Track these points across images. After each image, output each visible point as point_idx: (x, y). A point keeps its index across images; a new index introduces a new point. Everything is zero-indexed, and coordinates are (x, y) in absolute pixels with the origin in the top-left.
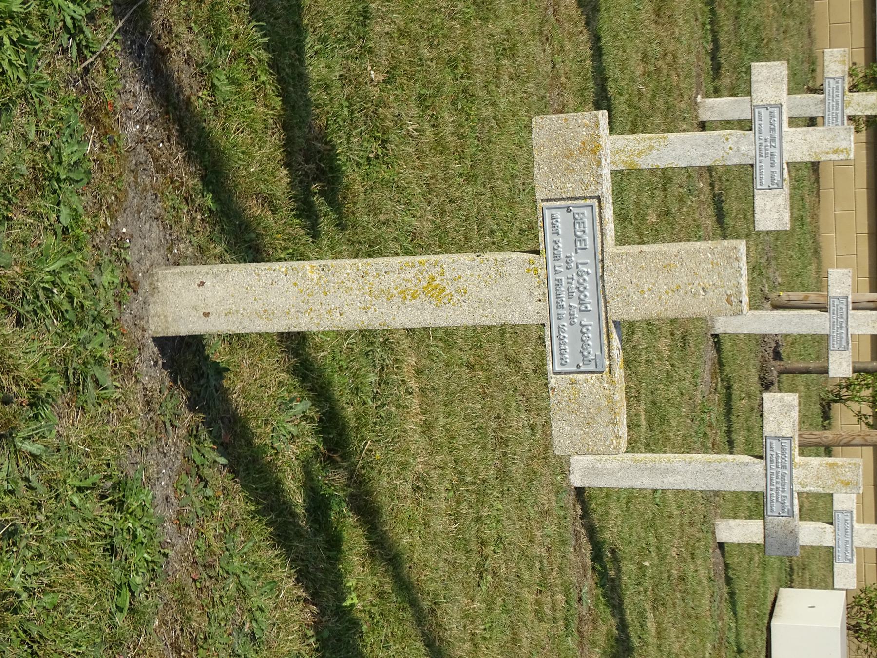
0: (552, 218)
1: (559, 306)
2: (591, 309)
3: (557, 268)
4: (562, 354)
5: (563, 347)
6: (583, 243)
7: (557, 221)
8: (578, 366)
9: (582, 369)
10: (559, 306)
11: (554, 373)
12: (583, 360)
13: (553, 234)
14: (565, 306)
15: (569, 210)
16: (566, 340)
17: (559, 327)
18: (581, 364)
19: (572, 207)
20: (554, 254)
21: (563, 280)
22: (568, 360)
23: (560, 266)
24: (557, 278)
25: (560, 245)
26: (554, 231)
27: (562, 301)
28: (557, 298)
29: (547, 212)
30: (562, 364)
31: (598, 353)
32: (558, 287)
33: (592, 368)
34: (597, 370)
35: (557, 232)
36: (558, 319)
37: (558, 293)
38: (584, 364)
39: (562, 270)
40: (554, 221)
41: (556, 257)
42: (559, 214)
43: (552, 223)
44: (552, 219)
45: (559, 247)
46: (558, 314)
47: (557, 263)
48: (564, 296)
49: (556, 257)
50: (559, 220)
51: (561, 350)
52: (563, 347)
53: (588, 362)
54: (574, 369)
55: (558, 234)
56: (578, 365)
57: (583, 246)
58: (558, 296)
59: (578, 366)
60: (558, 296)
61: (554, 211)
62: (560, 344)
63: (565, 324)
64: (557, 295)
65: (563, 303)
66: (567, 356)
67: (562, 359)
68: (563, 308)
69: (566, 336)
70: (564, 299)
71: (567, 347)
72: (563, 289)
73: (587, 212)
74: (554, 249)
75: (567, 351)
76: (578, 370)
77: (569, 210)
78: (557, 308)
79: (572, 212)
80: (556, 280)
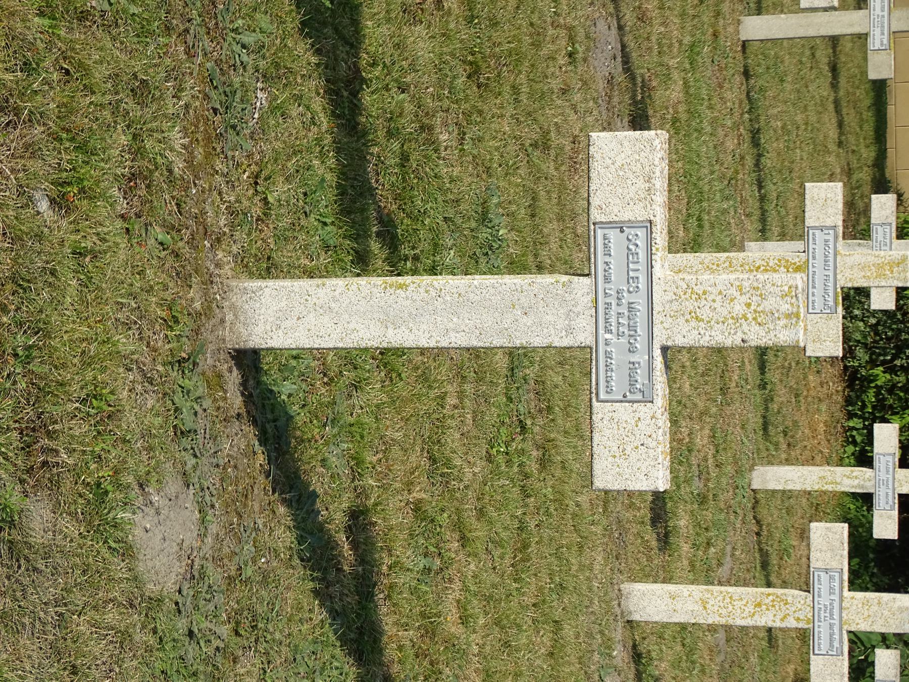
0: (605, 238)
2: (641, 333)
3: (607, 291)
4: (607, 382)
5: (609, 374)
6: (636, 256)
7: (610, 242)
8: (625, 396)
9: (630, 397)
11: (598, 401)
13: (605, 255)
14: (613, 331)
15: (622, 231)
18: (628, 394)
20: (605, 276)
21: (613, 304)
22: (614, 388)
23: (610, 289)
24: (607, 301)
25: (612, 266)
27: (611, 325)
29: (600, 233)
30: (607, 392)
31: (647, 382)
34: (645, 399)
36: (606, 344)
37: (607, 317)
38: (630, 392)
41: (607, 279)
42: (613, 234)
43: (605, 244)
44: (605, 239)
47: (607, 286)
48: (613, 320)
50: (611, 241)
51: (607, 377)
52: (609, 374)
54: (621, 398)
55: (610, 255)
56: (625, 394)
57: (635, 260)
58: (606, 321)
59: (624, 397)
60: (606, 321)
61: (606, 231)
62: (607, 371)
63: (613, 350)
64: (606, 319)
66: (613, 384)
67: (607, 387)
69: (613, 362)
70: (613, 324)
71: (613, 374)
73: (641, 233)
74: (605, 271)
75: (614, 378)
77: (622, 231)
79: (625, 235)
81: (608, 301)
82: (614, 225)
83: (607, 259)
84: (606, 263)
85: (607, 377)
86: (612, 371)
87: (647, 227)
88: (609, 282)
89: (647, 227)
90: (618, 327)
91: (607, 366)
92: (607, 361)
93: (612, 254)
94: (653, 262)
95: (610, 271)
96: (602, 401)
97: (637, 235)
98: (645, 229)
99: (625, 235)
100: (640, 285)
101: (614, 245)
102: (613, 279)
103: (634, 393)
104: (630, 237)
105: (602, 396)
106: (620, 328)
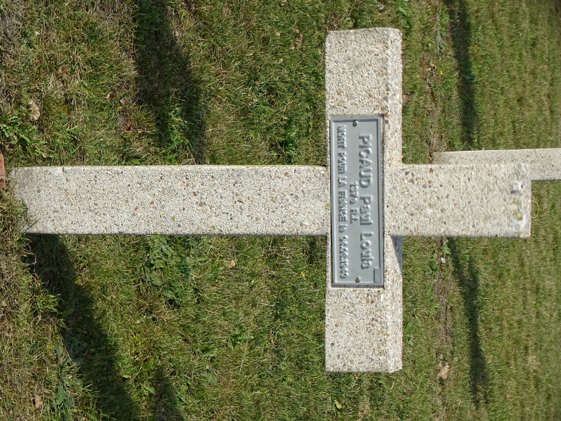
0: (339, 131)
2: (372, 221)
3: (341, 181)
4: (341, 267)
5: (343, 260)
7: (343, 134)
8: (357, 281)
11: (333, 286)
13: (339, 147)
14: (347, 219)
15: (355, 125)
16: (347, 254)
20: (339, 166)
22: (347, 274)
23: (344, 179)
25: (345, 158)
26: (340, 145)
27: (344, 213)
28: (340, 211)
29: (334, 125)
32: (340, 199)
35: (342, 145)
36: (341, 232)
37: (341, 205)
39: (346, 183)
40: (340, 133)
41: (340, 170)
42: (345, 127)
43: (338, 136)
44: (338, 132)
45: (343, 159)
46: (340, 227)
47: (341, 176)
48: (346, 209)
49: (340, 170)
50: (345, 133)
52: (343, 260)
54: (353, 282)
55: (343, 147)
58: (340, 209)
61: (340, 124)
62: (340, 257)
63: (347, 237)
64: (340, 207)
65: (345, 215)
66: (347, 269)
67: (341, 272)
68: (345, 220)
69: (347, 249)
70: (346, 212)
71: (347, 260)
72: (346, 202)
74: (339, 162)
75: (347, 264)
77: (355, 125)
78: (339, 220)
80: (340, 193)
81: (341, 190)
84: (340, 155)
85: (341, 263)
86: (345, 257)
88: (342, 173)
89: (377, 120)
91: (340, 252)
92: (341, 248)
93: (345, 146)
98: (375, 123)
100: (370, 149)
101: (347, 138)
102: (346, 169)
105: (336, 281)
106: (353, 216)
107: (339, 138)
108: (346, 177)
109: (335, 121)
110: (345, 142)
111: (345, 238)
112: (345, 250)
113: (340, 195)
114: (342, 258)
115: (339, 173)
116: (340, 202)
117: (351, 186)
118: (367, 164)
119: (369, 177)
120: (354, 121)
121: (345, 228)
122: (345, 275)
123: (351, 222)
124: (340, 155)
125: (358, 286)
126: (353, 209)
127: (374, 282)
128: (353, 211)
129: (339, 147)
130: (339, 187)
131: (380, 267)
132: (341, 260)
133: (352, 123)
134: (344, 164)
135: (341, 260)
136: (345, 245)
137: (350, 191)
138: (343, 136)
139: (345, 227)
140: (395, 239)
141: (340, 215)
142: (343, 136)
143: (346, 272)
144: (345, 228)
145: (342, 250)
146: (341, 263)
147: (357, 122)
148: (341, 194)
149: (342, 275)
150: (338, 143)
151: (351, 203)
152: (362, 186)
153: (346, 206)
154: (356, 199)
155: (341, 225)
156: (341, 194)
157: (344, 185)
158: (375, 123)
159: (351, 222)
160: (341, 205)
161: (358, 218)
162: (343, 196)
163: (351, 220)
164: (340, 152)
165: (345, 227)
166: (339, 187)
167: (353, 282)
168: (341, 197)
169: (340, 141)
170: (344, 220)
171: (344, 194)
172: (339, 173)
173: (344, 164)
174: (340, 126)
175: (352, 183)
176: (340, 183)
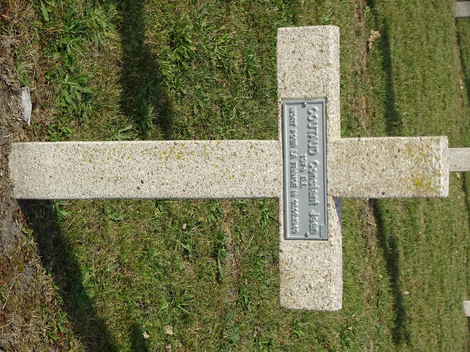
0: (290, 111)
1: (293, 185)
3: (292, 154)
4: (293, 224)
5: (294, 219)
7: (294, 115)
8: (306, 235)
9: (310, 237)
10: (293, 185)
12: (310, 231)
13: (291, 125)
14: (297, 185)
15: (304, 106)
16: (297, 213)
17: (292, 203)
18: (308, 234)
19: (308, 103)
20: (290, 142)
21: (297, 164)
22: (298, 230)
23: (294, 152)
24: (292, 162)
25: (296, 134)
26: (291, 123)
27: (295, 181)
28: (292, 178)
29: (286, 107)
30: (293, 233)
31: (323, 224)
32: (292, 169)
33: (318, 237)
35: (293, 123)
36: (292, 196)
37: (292, 174)
38: (311, 234)
39: (296, 155)
40: (292, 114)
41: (292, 144)
42: (295, 109)
43: (290, 116)
45: (294, 135)
46: (292, 192)
47: (292, 150)
48: (297, 177)
50: (296, 114)
53: (314, 232)
54: (303, 237)
55: (294, 125)
56: (307, 234)
58: (292, 177)
59: (306, 235)
60: (292, 177)
61: (291, 106)
62: (292, 216)
63: (297, 200)
64: (291, 176)
66: (297, 226)
67: (293, 228)
68: (296, 187)
69: (297, 209)
70: (297, 179)
71: (297, 218)
72: (297, 171)
74: (291, 138)
75: (298, 221)
76: (306, 238)
77: (304, 106)
78: (291, 187)
82: (298, 101)
83: (292, 128)
84: (291, 132)
85: (292, 220)
86: (295, 216)
87: (322, 103)
88: (294, 147)
90: (301, 181)
91: (292, 212)
92: (292, 208)
93: (296, 124)
94: (328, 137)
95: (295, 137)
96: (289, 240)
97: (314, 110)
98: (321, 105)
99: (305, 110)
101: (297, 117)
103: (314, 234)
104: (310, 111)
105: (288, 236)
106: (302, 182)
107: (291, 118)
108: (296, 150)
109: (288, 104)
110: (296, 121)
111: (295, 201)
112: (296, 210)
113: (292, 165)
114: (294, 217)
115: (291, 147)
116: (291, 172)
117: (301, 157)
118: (314, 139)
119: (316, 147)
120: (303, 103)
121: (296, 193)
122: (296, 231)
123: (301, 187)
124: (291, 132)
125: (306, 240)
126: (302, 176)
127: (320, 236)
128: (302, 178)
129: (291, 125)
130: (291, 159)
131: (325, 224)
132: (292, 218)
133: (301, 105)
134: (295, 140)
135: (292, 218)
136: (296, 206)
137: (300, 161)
138: (294, 116)
139: (296, 192)
140: (338, 201)
141: (291, 182)
142: (294, 116)
143: (296, 228)
144: (296, 193)
145: (293, 210)
146: (292, 220)
147: (306, 103)
148: (293, 165)
149: (293, 231)
150: (290, 122)
151: (301, 171)
152: (309, 154)
153: (297, 174)
154: (305, 168)
155: (293, 190)
156: (293, 165)
157: (295, 157)
158: (321, 105)
159: (301, 187)
160: (292, 174)
161: (307, 183)
162: (294, 166)
163: (301, 185)
164: (291, 129)
165: (296, 192)
166: (291, 159)
167: (303, 237)
168: (293, 167)
169: (291, 121)
170: (295, 186)
171: (295, 165)
172: (291, 147)
173: (295, 140)
174: (291, 108)
175: (301, 155)
176: (291, 155)
